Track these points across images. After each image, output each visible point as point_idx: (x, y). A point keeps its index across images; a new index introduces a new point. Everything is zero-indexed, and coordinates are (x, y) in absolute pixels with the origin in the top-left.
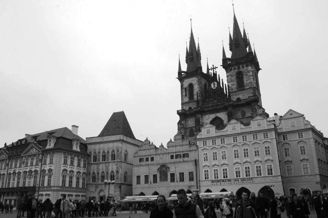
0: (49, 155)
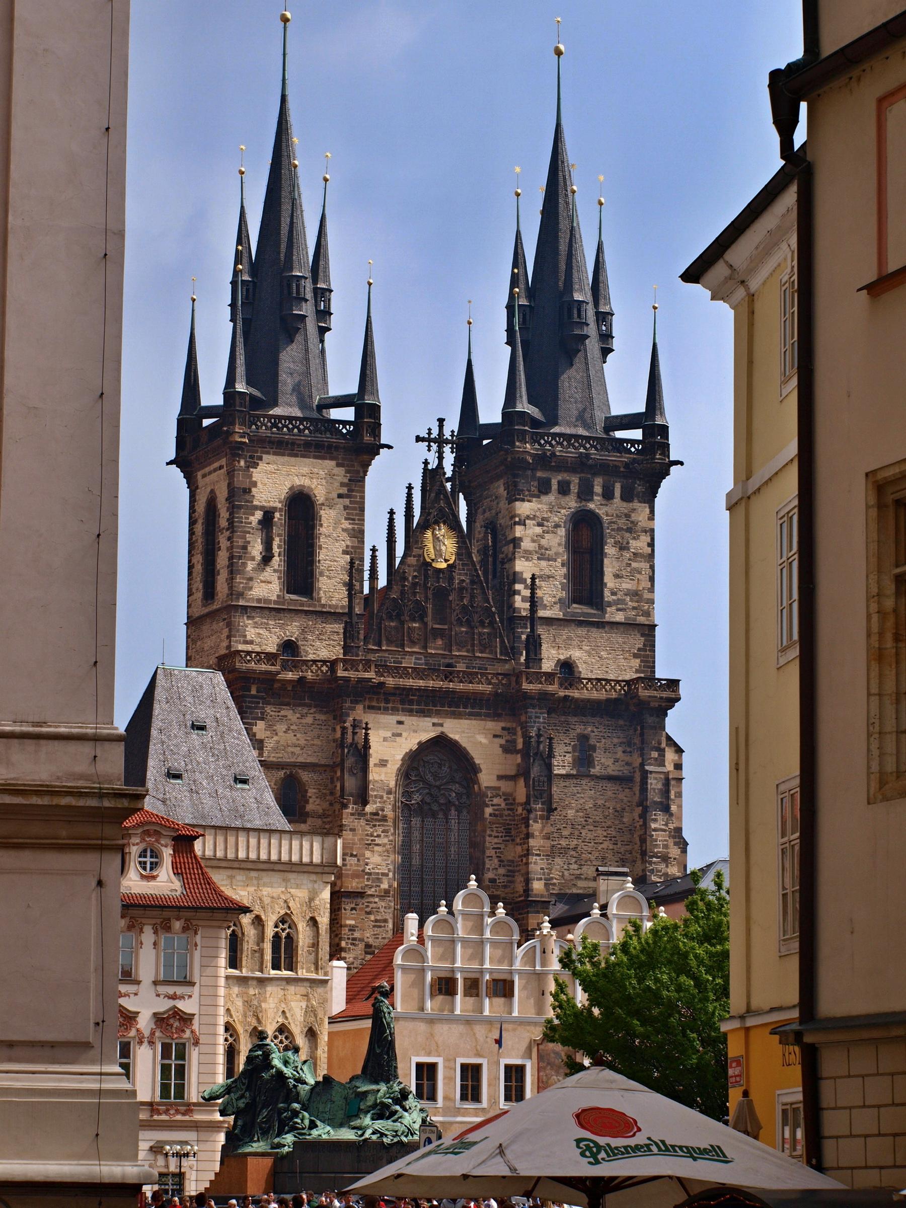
0: (148, 931)
